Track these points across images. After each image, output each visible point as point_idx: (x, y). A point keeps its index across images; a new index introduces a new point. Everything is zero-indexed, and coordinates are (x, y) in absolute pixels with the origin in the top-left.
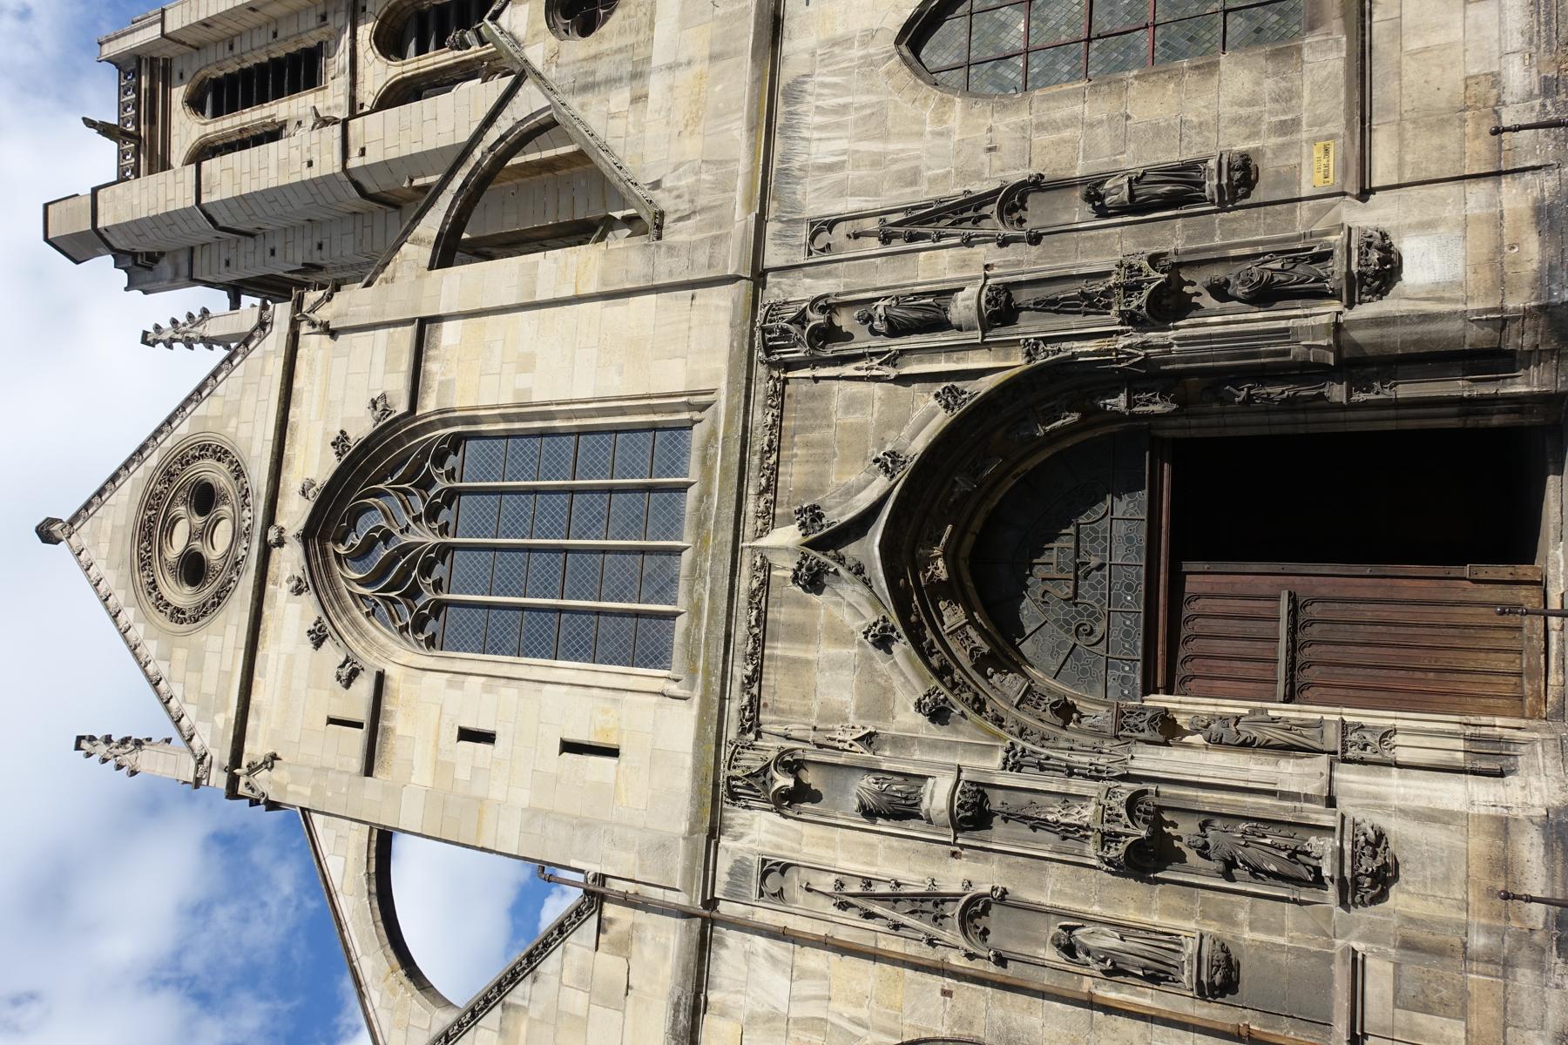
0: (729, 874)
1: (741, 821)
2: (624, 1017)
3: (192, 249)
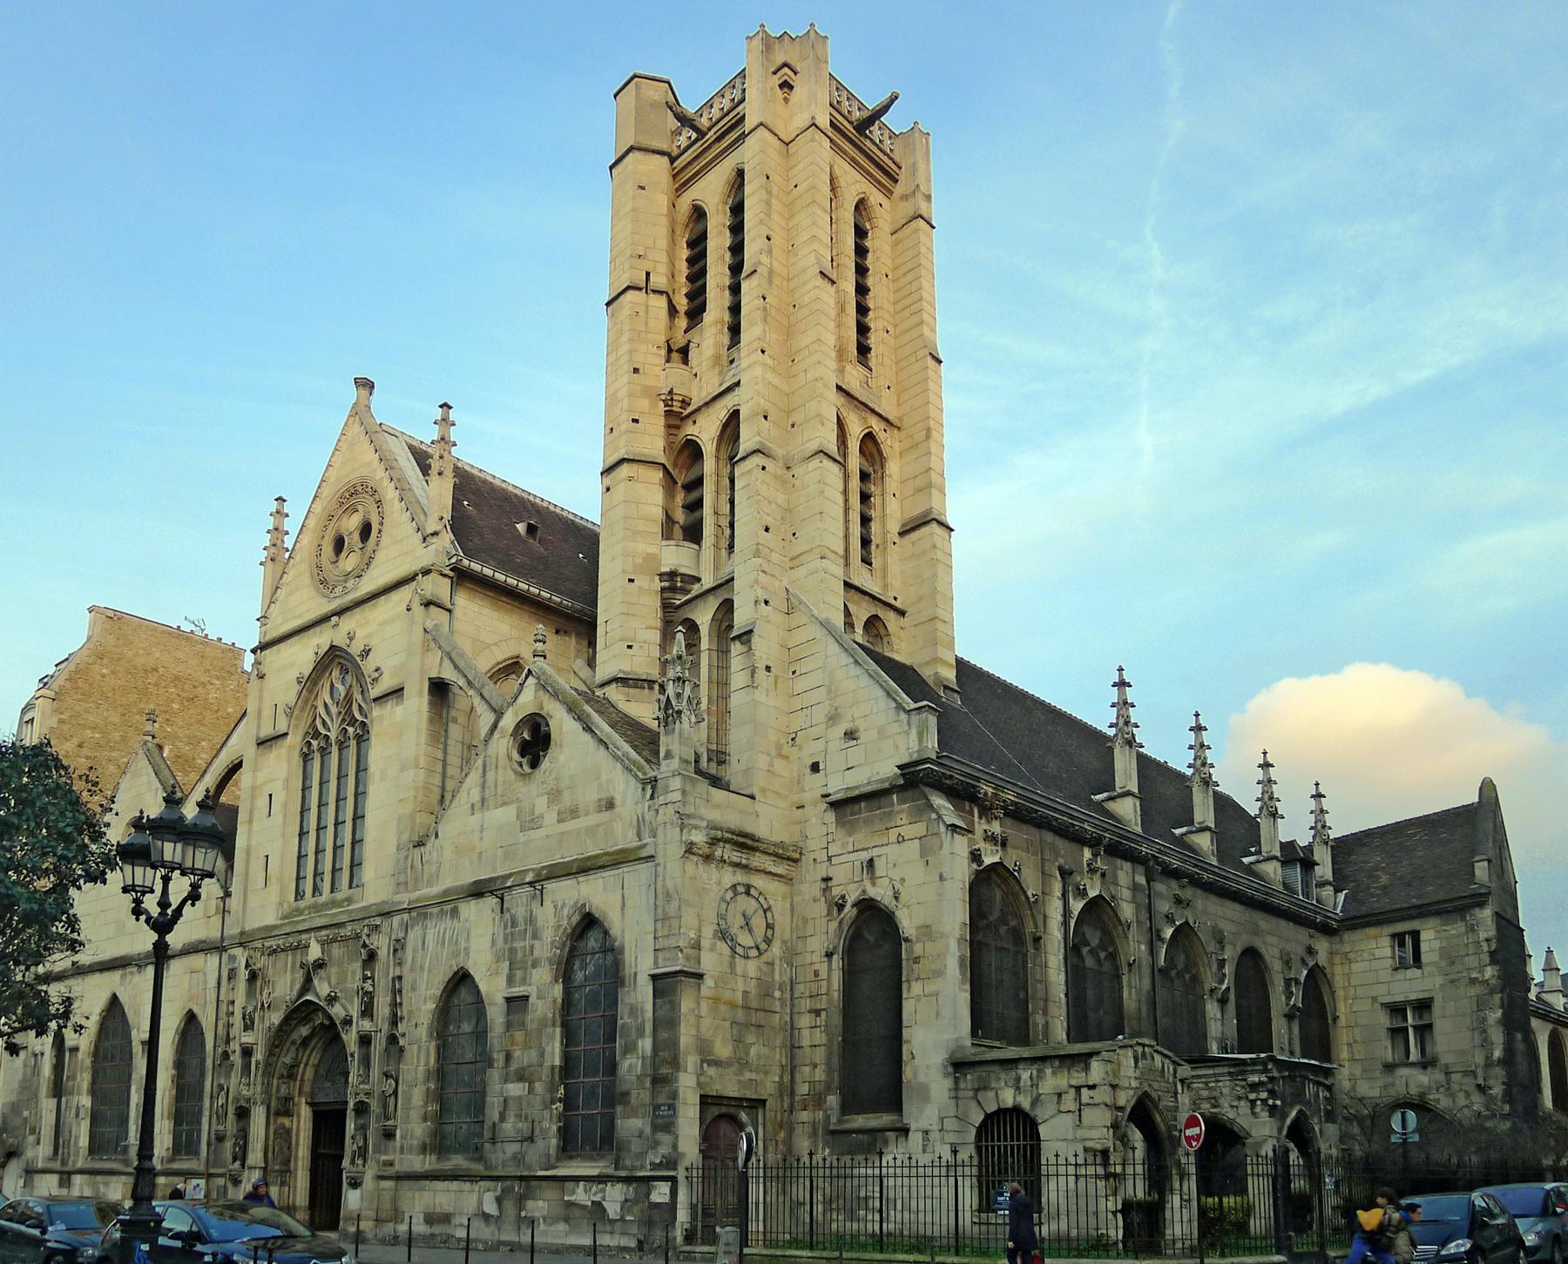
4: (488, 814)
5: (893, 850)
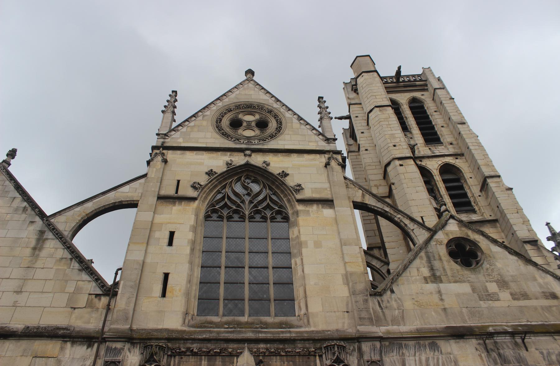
0: (115, 348)
1: (136, 351)
2: (64, 307)
3: (360, 104)
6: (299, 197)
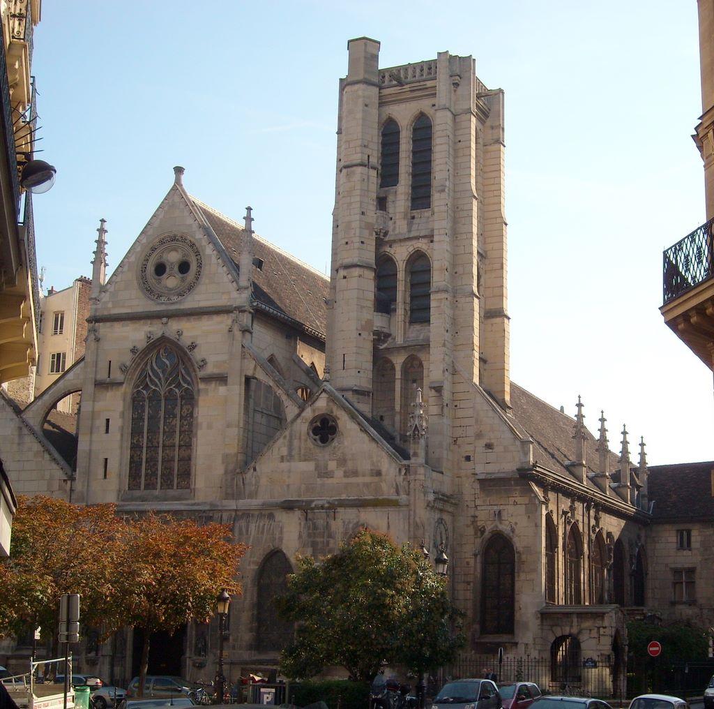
4: (293, 464)
5: (511, 509)
6: (201, 374)
